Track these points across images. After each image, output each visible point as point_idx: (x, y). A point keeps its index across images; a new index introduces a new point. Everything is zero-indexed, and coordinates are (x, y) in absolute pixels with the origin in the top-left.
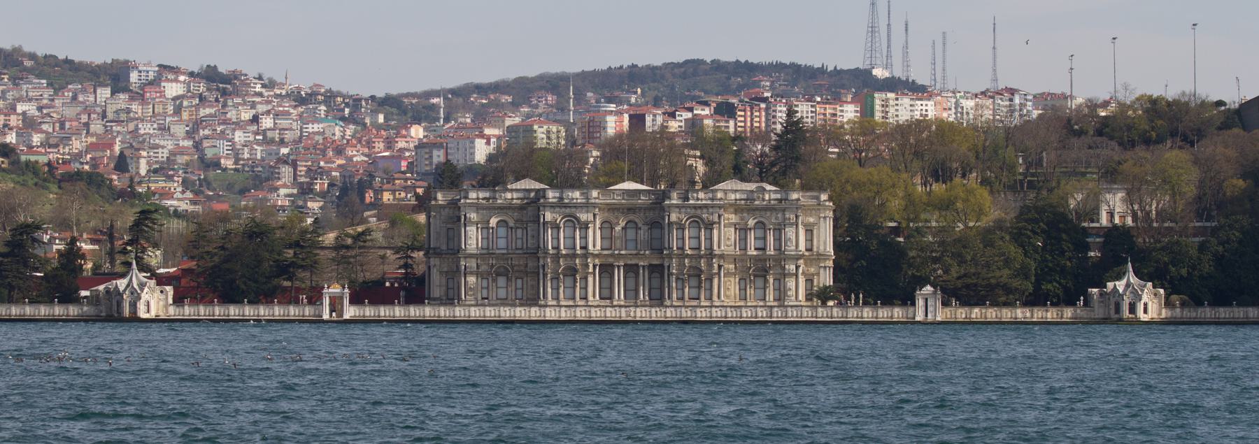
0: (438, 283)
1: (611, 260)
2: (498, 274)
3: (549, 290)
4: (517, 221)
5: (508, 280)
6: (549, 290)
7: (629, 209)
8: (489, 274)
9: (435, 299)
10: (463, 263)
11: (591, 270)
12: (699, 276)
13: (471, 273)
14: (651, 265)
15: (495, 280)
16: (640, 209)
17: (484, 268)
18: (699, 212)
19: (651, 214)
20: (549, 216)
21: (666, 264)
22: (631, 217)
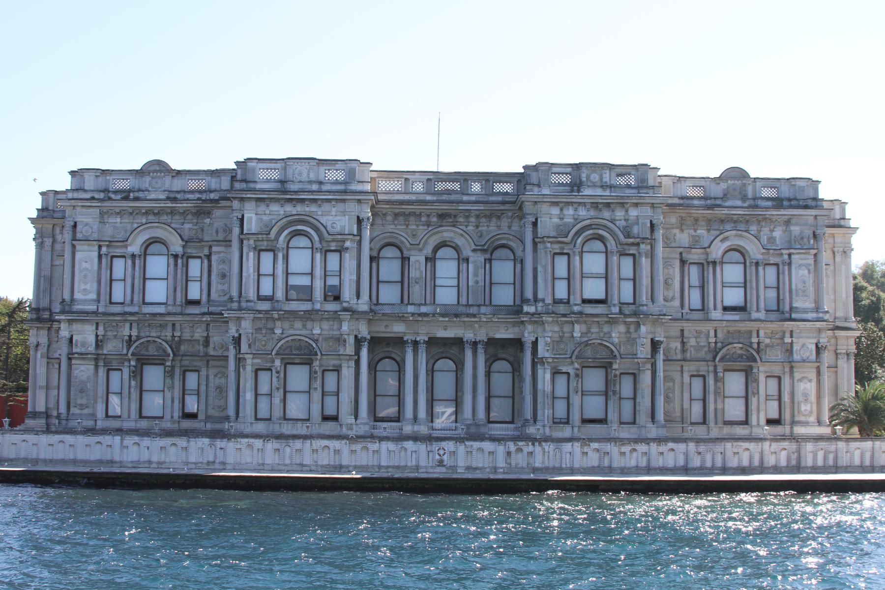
0: (42, 381)
1: (398, 328)
2: (143, 361)
3: (249, 396)
4: (187, 242)
5: (169, 374)
6: (248, 396)
7: (442, 216)
8: (123, 358)
9: (35, 415)
10: (64, 333)
11: (350, 349)
12: (607, 367)
13: (83, 356)
14: (492, 343)
15: (137, 374)
16: (467, 214)
17: (110, 347)
18: (606, 214)
19: (490, 228)
20: (253, 219)
21: (528, 338)
22: (447, 234)
